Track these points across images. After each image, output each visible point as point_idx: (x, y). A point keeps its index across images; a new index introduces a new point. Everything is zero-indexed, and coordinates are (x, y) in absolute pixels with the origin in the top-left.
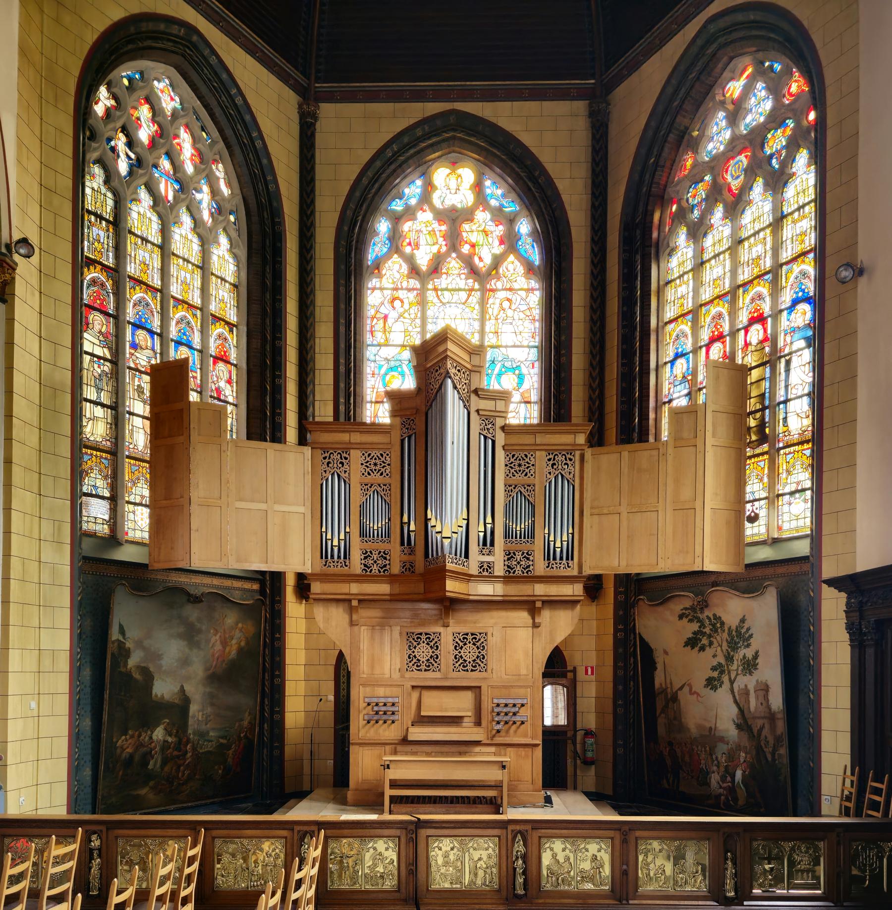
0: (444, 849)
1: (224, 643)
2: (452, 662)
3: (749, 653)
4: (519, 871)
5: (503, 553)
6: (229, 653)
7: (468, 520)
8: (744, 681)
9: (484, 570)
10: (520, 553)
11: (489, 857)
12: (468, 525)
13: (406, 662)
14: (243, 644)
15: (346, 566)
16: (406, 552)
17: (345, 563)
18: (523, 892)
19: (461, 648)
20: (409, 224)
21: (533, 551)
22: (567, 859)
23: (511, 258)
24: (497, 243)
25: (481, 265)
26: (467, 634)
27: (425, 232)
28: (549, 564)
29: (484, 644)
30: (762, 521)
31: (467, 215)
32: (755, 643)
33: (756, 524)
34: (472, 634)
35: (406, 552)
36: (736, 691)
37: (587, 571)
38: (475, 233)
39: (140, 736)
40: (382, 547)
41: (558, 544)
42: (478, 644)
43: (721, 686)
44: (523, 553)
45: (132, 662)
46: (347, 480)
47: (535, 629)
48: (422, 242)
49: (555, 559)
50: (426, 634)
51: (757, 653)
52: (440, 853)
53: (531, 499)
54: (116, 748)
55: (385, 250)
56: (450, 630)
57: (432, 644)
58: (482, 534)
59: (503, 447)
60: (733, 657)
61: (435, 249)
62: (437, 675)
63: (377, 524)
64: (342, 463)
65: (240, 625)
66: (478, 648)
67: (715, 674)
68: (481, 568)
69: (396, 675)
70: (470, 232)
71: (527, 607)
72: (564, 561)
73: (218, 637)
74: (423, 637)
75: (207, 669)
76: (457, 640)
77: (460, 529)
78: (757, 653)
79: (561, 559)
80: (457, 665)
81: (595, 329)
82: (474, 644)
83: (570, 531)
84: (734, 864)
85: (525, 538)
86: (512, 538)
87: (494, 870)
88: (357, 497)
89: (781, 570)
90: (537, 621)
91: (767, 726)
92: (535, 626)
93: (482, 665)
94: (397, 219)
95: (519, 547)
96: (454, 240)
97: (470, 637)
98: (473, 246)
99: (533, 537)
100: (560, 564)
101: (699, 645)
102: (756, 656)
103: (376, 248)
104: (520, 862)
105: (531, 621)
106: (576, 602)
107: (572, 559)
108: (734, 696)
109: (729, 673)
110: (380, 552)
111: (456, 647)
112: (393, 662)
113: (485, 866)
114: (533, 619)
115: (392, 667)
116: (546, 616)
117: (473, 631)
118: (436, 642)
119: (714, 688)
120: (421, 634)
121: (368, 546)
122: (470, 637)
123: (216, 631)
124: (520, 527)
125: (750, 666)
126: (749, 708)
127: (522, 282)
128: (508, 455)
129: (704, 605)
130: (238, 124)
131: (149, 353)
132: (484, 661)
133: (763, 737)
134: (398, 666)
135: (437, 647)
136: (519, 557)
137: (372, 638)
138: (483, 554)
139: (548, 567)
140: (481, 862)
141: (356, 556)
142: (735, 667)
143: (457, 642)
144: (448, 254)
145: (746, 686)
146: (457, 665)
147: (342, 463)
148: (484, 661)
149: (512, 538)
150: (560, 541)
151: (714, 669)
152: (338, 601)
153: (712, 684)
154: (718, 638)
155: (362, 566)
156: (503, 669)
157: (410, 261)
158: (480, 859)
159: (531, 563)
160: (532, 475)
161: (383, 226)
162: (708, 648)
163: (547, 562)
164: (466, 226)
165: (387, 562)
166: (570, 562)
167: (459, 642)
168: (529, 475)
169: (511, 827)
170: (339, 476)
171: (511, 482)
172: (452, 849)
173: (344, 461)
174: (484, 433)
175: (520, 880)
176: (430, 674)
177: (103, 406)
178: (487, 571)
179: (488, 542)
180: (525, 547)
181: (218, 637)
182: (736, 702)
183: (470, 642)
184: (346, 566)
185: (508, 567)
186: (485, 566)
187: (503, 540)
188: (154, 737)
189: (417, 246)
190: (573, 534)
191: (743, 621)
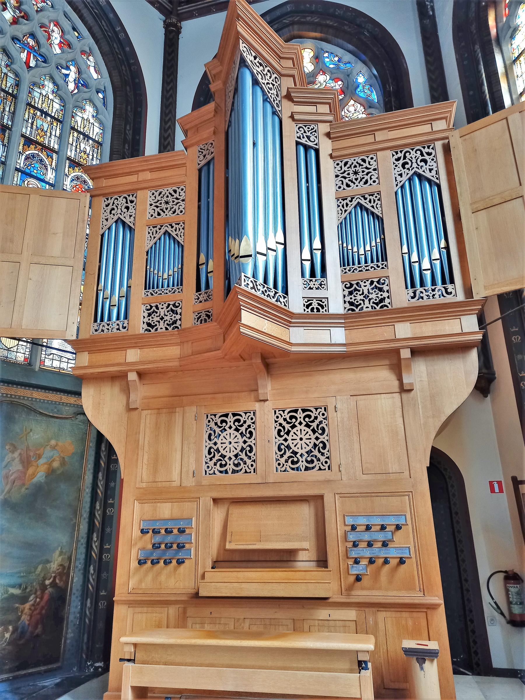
2: (275, 456)
5: (341, 286)
7: (285, 244)
9: (312, 310)
10: (368, 283)
12: (285, 249)
13: (204, 460)
15: (125, 328)
16: (201, 299)
19: (288, 433)
21: (387, 277)
26: (296, 411)
28: (415, 293)
29: (323, 425)
34: (304, 411)
35: (201, 299)
40: (171, 298)
42: (314, 425)
44: (372, 283)
46: (132, 225)
47: (405, 396)
49: (422, 284)
50: (234, 415)
53: (376, 211)
56: (269, 406)
57: (243, 429)
59: (331, 156)
62: (252, 478)
66: (314, 431)
68: (308, 307)
71: (387, 362)
72: (440, 286)
74: (231, 419)
76: (281, 420)
77: (271, 254)
80: (282, 460)
82: (308, 426)
83: (443, 244)
85: (372, 262)
86: (353, 264)
90: (406, 380)
92: (404, 390)
93: (323, 459)
95: (365, 275)
97: (300, 415)
99: (385, 258)
100: (433, 290)
105: (396, 383)
107: (452, 281)
110: (169, 305)
111: (279, 431)
112: (185, 460)
114: (400, 379)
115: (184, 470)
117: (306, 405)
118: (249, 426)
120: (226, 415)
122: (300, 415)
128: (338, 164)
130: (103, 21)
132: (325, 451)
134: (193, 467)
135: (251, 433)
136: (366, 288)
137: (157, 426)
138: (310, 288)
139: (413, 298)
143: (281, 425)
146: (282, 460)
147: (127, 208)
148: (325, 451)
149: (353, 264)
155: (145, 326)
156: (358, 463)
159: (385, 295)
160: (374, 182)
163: (411, 291)
165: (178, 317)
166: (450, 287)
167: (284, 423)
168: (370, 182)
171: (344, 194)
173: (129, 204)
174: (303, 141)
176: (240, 477)
180: (375, 274)
183: (300, 423)
185: (351, 304)
186: (315, 305)
187: (339, 269)
190: (447, 248)
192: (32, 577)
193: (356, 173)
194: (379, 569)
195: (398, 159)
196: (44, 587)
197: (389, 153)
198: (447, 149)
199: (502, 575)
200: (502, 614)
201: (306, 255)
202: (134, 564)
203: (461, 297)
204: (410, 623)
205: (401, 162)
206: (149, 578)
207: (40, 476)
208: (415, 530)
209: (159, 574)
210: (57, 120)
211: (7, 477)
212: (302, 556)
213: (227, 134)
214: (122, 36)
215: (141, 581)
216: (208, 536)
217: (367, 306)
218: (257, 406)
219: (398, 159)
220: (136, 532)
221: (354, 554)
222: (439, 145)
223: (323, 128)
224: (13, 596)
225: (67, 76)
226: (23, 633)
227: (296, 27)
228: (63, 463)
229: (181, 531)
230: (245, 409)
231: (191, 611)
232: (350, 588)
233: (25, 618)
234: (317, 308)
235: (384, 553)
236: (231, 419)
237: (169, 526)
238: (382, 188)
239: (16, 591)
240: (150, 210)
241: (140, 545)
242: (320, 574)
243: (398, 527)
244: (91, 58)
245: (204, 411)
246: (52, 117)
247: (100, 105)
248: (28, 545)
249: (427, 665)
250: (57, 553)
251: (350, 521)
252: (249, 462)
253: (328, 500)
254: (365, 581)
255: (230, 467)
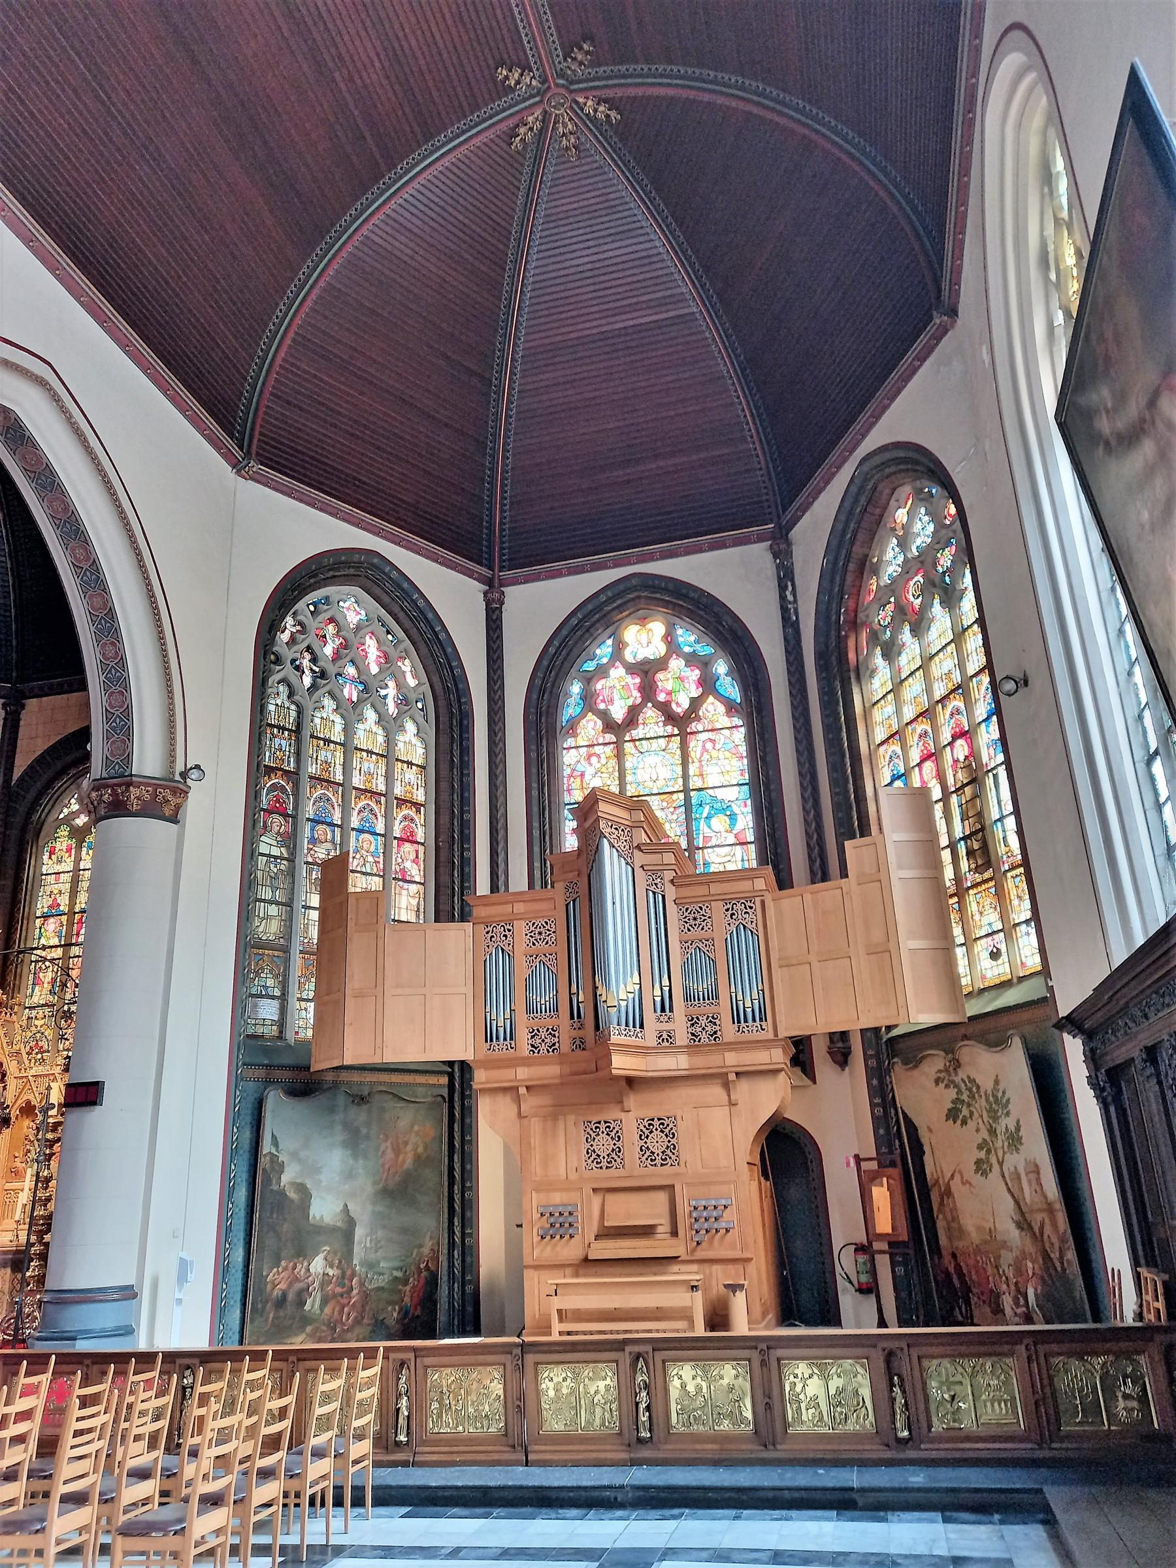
0: (555, 1380)
1: (397, 1151)
3: (1010, 1122)
4: (643, 1406)
6: (404, 1162)
8: (1014, 1161)
11: (608, 1388)
14: (420, 1150)
18: (649, 1435)
20: (602, 682)
22: (699, 1389)
23: (711, 699)
24: (693, 687)
25: (679, 710)
27: (618, 687)
30: (1004, 957)
31: (661, 664)
33: (1000, 961)
36: (1007, 1175)
37: (782, 1033)
38: (671, 681)
39: (294, 1268)
40: (550, 1023)
41: (748, 1004)
42: (667, 1131)
45: (285, 1178)
47: (733, 1108)
48: (616, 697)
49: (746, 1021)
51: (1018, 1122)
52: (551, 1385)
54: (266, 1283)
55: (578, 710)
58: (658, 999)
61: (630, 702)
62: (621, 1172)
63: (544, 998)
64: (505, 936)
65: (416, 1128)
67: (982, 1154)
69: (573, 1176)
70: (666, 682)
71: (720, 1081)
73: (389, 1143)
74: (603, 1126)
75: (375, 1183)
77: (631, 996)
78: (1018, 1122)
79: (754, 1020)
80: (644, 1159)
81: (802, 760)
84: (904, 1392)
87: (614, 1406)
88: (522, 969)
89: (1026, 1015)
92: (732, 1104)
94: (588, 679)
96: (648, 690)
97: (656, 1123)
98: (669, 693)
102: (1018, 1128)
103: (571, 708)
104: (644, 1394)
106: (776, 1072)
108: (1007, 1184)
113: (603, 1401)
114: (729, 1096)
116: (743, 1089)
121: (535, 1024)
122: (656, 1123)
123: (387, 1137)
124: (702, 986)
125: (1015, 1140)
127: (725, 721)
129: (957, 1064)
131: (329, 845)
134: (575, 1164)
136: (703, 1021)
140: (599, 1397)
141: (523, 1036)
142: (999, 1144)
144: (643, 705)
146: (644, 1159)
147: (505, 936)
150: (749, 1001)
152: (505, 1090)
153: (981, 1167)
154: (977, 1106)
157: (604, 716)
158: (596, 1392)
159: (718, 1028)
161: (576, 688)
164: (660, 676)
166: (764, 1024)
169: (628, 1349)
170: (503, 950)
172: (564, 1380)
175: (644, 1418)
177: (278, 903)
179: (665, 1007)
180: (710, 1010)
181: (389, 1143)
185: (693, 1034)
186: (665, 1036)
188: (312, 1270)
189: (611, 701)
191: (997, 1082)
192: (410, 1260)
193: (695, 919)
194: (713, 1237)
195: (727, 910)
196: (420, 1271)
197: (722, 903)
198: (763, 903)
199: (854, 1247)
200: (851, 1282)
201: (658, 992)
202: (537, 1239)
203: (771, 1036)
204: (733, 1272)
205: (730, 912)
206: (549, 1248)
207: (409, 1162)
208: (738, 1208)
209: (555, 1246)
210: (382, 756)
211: (383, 1165)
212: (660, 1229)
213: (589, 876)
214: (442, 636)
215: (542, 1251)
216: (590, 1217)
217: (704, 1037)
218: (623, 1115)
219: (727, 910)
220: (536, 1216)
221: (696, 1226)
222: (758, 900)
223: (669, 875)
224: (396, 1278)
225: (385, 697)
226: (407, 1313)
227: (642, 601)
228: (426, 1148)
229: (571, 1214)
230: (614, 1117)
231: (581, 1271)
232: (694, 1251)
233: (407, 1299)
235: (716, 1226)
236: (603, 1126)
237: (560, 1209)
238: (715, 934)
239: (399, 1274)
240: (525, 939)
241: (538, 1225)
242: (674, 1241)
243: (725, 1207)
244: (407, 662)
245: (582, 1119)
246: (377, 754)
247: (421, 720)
248: (404, 1230)
249: (738, 1293)
250: (428, 1238)
251: (693, 1203)
252: (619, 1160)
253: (678, 1188)
254: (704, 1245)
255: (604, 1164)
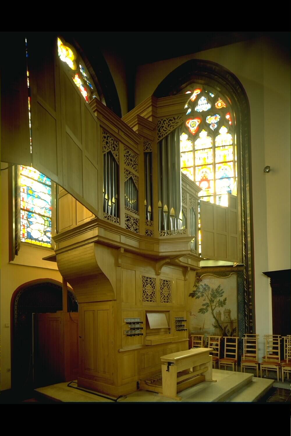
9: (148, 234)
17: (117, 220)
32: (225, 295)
43: (207, 312)
60: (214, 300)
67: (205, 307)
91: (229, 325)
101: (196, 296)
102: (225, 300)
108: (214, 315)
109: (211, 307)
119: (204, 313)
125: (222, 303)
126: (221, 319)
133: (227, 330)
142: (215, 304)
145: (219, 311)
151: (204, 305)
162: (201, 298)
178: (150, 236)
182: (214, 317)
184: (118, 222)
191: (219, 287)
234: (150, 234)
